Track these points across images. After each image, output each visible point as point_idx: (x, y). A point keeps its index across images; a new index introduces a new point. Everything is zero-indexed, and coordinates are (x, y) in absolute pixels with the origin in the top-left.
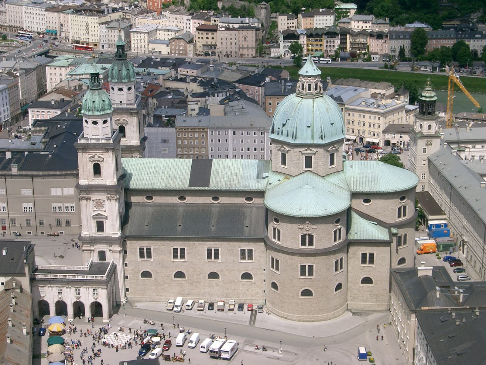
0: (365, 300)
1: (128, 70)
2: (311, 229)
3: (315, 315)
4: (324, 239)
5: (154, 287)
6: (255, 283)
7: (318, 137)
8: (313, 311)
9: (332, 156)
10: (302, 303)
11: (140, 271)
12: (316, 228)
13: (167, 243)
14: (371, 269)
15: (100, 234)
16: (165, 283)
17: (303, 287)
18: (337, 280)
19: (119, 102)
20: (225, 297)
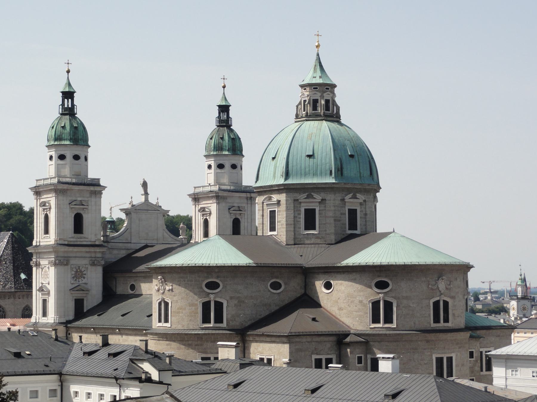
7: (279, 175)
9: (310, 215)
19: (208, 185)
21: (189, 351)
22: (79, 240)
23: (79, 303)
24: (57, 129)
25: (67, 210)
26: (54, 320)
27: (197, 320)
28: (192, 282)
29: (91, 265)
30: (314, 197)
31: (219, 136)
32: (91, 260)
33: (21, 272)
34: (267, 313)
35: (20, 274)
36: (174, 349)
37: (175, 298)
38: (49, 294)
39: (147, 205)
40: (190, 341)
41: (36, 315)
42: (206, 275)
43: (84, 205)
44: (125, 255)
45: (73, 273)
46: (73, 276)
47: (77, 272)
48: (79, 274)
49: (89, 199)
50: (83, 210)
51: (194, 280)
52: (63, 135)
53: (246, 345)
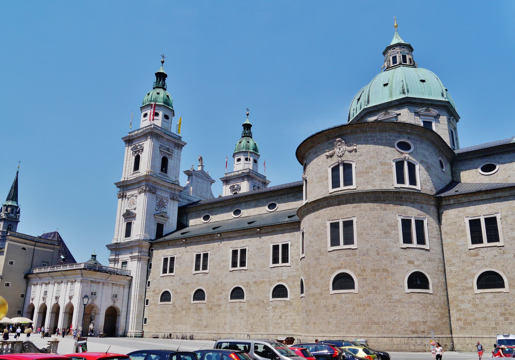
0: (494, 328)
1: (248, 142)
2: (347, 153)
3: (361, 332)
4: (374, 171)
5: (171, 315)
6: (291, 304)
8: (356, 324)
10: (334, 306)
11: (160, 291)
12: (356, 151)
13: (191, 249)
14: (495, 252)
15: (128, 240)
16: (183, 309)
17: (334, 269)
18: (411, 262)
20: (251, 331)
21: (386, 211)
22: (164, 177)
23: (160, 227)
24: (153, 94)
25: (158, 152)
26: (140, 237)
27: (391, 180)
28: (382, 140)
29: (171, 199)
30: (431, 111)
31: (246, 141)
32: (171, 195)
33: (61, 255)
34: (444, 186)
35: (61, 256)
36: (365, 211)
37: (361, 158)
38: (134, 216)
39: (203, 172)
40: (387, 200)
41: (118, 237)
42: (397, 134)
43: (170, 152)
44: (187, 204)
45: (158, 202)
46: (157, 204)
47: (160, 201)
48: (161, 204)
49: (173, 149)
50: (169, 155)
51: (385, 139)
52: (158, 99)
53: (441, 211)
